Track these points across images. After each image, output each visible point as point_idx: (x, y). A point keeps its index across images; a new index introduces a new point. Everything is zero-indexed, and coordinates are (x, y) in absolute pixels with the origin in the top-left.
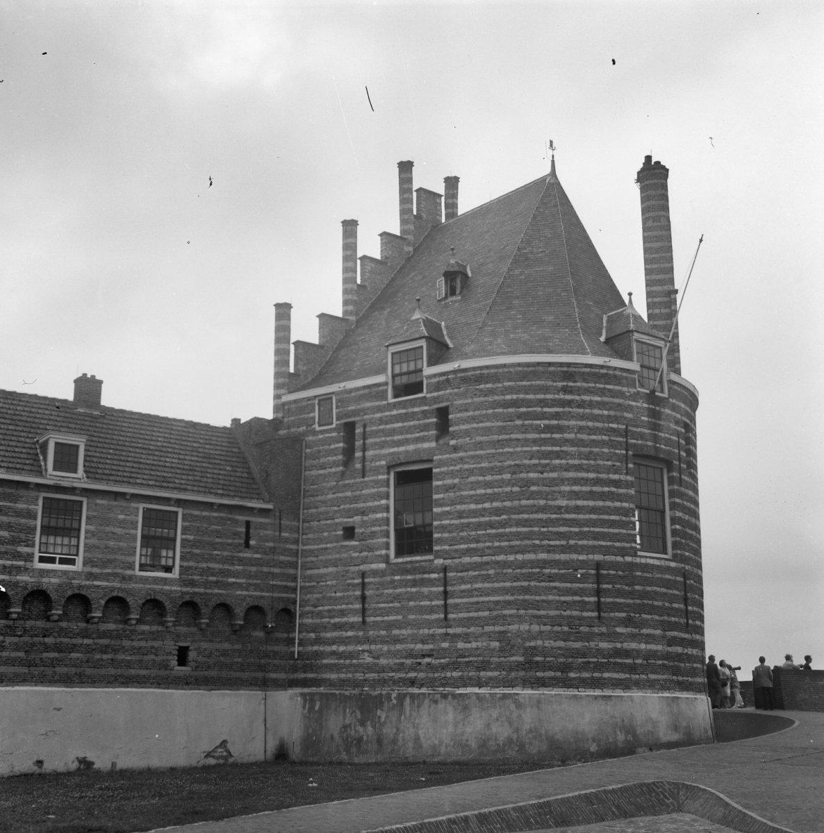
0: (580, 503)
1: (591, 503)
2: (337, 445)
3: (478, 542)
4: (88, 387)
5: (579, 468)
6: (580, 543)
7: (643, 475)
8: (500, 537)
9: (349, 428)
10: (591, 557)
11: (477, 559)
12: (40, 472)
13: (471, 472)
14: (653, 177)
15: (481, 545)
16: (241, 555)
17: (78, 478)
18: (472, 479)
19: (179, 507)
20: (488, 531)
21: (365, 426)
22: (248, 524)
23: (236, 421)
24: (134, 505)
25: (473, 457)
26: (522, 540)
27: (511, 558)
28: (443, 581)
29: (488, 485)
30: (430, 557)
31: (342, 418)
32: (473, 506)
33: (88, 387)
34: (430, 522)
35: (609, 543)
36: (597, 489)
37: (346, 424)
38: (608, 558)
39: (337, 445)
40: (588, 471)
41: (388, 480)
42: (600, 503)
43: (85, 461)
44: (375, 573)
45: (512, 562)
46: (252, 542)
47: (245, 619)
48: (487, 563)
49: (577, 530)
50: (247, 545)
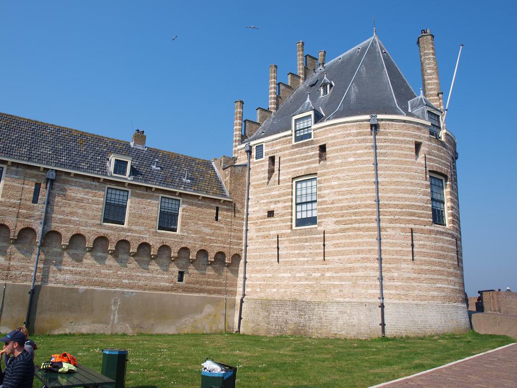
3: (342, 216)
4: (140, 136)
7: (433, 182)
8: (355, 214)
9: (272, 159)
10: (407, 225)
11: (344, 227)
15: (344, 218)
16: (213, 224)
17: (127, 178)
19: (180, 197)
20: (348, 211)
24: (156, 194)
26: (368, 215)
27: (362, 225)
30: (316, 226)
31: (268, 154)
33: (140, 136)
34: (316, 199)
35: (417, 218)
37: (270, 157)
41: (292, 185)
44: (284, 235)
45: (363, 228)
47: (214, 258)
48: (348, 229)
49: (400, 210)
50: (217, 219)
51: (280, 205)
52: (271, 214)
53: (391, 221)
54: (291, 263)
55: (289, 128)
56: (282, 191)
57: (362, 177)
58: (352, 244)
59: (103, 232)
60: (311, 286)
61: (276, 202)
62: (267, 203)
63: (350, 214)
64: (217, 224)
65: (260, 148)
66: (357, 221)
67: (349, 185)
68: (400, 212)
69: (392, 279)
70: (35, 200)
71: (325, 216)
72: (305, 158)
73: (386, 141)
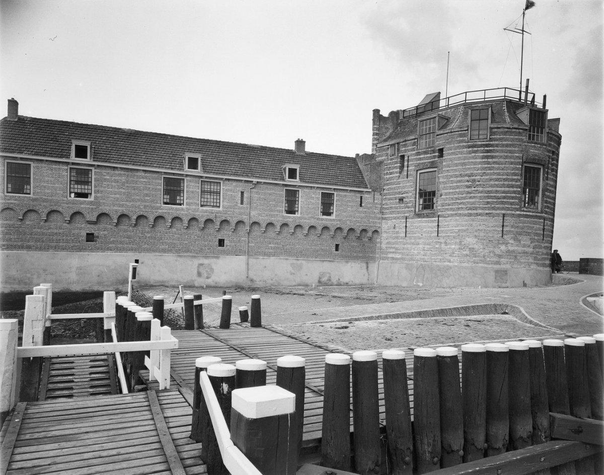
0: (499, 189)
1: (503, 189)
2: (397, 165)
4: (300, 143)
5: (499, 174)
6: (497, 206)
12: (283, 180)
13: (451, 176)
18: (452, 179)
21: (408, 157)
22: (361, 197)
23: (357, 155)
25: (452, 170)
28: (437, 221)
32: (451, 191)
33: (300, 143)
36: (506, 183)
38: (508, 212)
39: (397, 165)
40: (503, 175)
42: (507, 189)
43: (300, 174)
46: (363, 205)
50: (361, 205)
52: (401, 200)
59: (285, 221)
64: (361, 209)
68: (496, 202)
70: (242, 203)
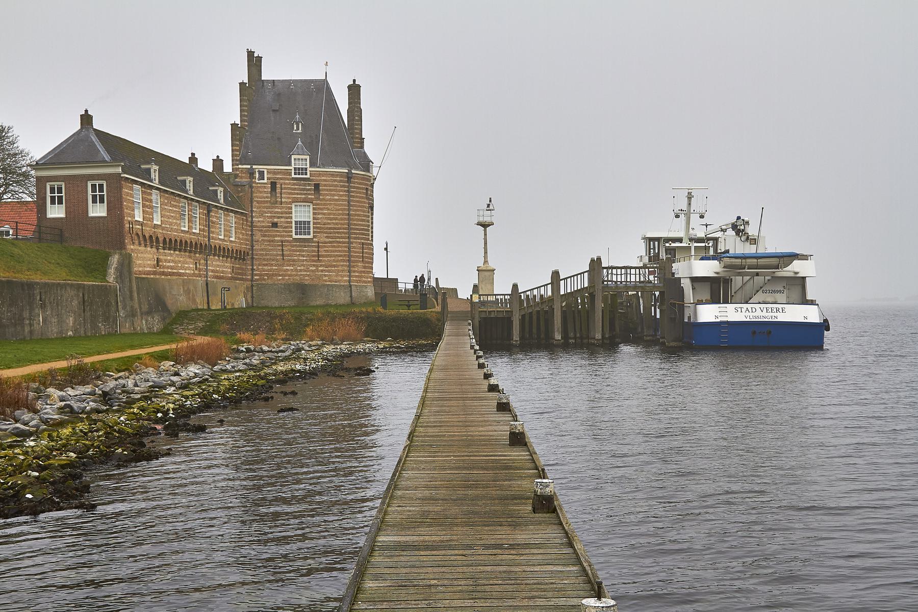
9: (273, 185)
14: (354, 90)
29: (334, 214)
33: (193, 159)
44: (288, 241)
51: (282, 220)
52: (275, 225)
53: (355, 238)
54: (294, 261)
55: (290, 165)
56: (284, 210)
57: (341, 210)
58: (336, 251)
60: (308, 275)
61: (279, 217)
62: (271, 217)
63: (335, 233)
65: (261, 174)
66: (339, 237)
67: (334, 214)
69: (354, 272)
71: (319, 232)
72: (303, 190)
73: (354, 187)
